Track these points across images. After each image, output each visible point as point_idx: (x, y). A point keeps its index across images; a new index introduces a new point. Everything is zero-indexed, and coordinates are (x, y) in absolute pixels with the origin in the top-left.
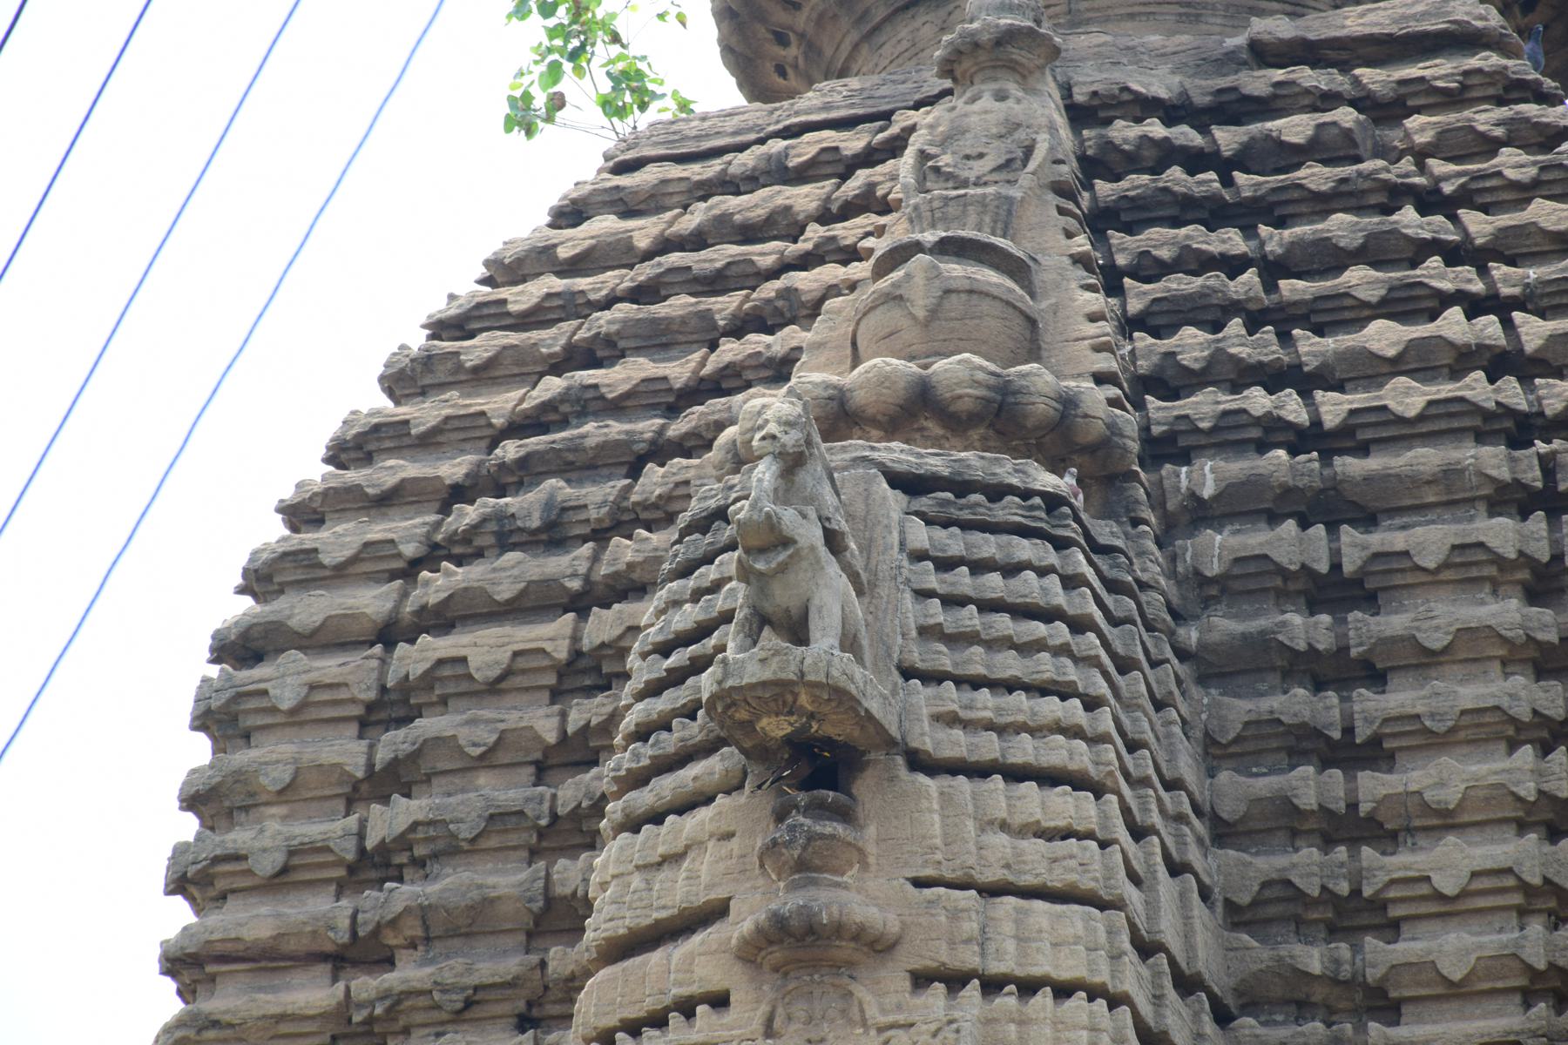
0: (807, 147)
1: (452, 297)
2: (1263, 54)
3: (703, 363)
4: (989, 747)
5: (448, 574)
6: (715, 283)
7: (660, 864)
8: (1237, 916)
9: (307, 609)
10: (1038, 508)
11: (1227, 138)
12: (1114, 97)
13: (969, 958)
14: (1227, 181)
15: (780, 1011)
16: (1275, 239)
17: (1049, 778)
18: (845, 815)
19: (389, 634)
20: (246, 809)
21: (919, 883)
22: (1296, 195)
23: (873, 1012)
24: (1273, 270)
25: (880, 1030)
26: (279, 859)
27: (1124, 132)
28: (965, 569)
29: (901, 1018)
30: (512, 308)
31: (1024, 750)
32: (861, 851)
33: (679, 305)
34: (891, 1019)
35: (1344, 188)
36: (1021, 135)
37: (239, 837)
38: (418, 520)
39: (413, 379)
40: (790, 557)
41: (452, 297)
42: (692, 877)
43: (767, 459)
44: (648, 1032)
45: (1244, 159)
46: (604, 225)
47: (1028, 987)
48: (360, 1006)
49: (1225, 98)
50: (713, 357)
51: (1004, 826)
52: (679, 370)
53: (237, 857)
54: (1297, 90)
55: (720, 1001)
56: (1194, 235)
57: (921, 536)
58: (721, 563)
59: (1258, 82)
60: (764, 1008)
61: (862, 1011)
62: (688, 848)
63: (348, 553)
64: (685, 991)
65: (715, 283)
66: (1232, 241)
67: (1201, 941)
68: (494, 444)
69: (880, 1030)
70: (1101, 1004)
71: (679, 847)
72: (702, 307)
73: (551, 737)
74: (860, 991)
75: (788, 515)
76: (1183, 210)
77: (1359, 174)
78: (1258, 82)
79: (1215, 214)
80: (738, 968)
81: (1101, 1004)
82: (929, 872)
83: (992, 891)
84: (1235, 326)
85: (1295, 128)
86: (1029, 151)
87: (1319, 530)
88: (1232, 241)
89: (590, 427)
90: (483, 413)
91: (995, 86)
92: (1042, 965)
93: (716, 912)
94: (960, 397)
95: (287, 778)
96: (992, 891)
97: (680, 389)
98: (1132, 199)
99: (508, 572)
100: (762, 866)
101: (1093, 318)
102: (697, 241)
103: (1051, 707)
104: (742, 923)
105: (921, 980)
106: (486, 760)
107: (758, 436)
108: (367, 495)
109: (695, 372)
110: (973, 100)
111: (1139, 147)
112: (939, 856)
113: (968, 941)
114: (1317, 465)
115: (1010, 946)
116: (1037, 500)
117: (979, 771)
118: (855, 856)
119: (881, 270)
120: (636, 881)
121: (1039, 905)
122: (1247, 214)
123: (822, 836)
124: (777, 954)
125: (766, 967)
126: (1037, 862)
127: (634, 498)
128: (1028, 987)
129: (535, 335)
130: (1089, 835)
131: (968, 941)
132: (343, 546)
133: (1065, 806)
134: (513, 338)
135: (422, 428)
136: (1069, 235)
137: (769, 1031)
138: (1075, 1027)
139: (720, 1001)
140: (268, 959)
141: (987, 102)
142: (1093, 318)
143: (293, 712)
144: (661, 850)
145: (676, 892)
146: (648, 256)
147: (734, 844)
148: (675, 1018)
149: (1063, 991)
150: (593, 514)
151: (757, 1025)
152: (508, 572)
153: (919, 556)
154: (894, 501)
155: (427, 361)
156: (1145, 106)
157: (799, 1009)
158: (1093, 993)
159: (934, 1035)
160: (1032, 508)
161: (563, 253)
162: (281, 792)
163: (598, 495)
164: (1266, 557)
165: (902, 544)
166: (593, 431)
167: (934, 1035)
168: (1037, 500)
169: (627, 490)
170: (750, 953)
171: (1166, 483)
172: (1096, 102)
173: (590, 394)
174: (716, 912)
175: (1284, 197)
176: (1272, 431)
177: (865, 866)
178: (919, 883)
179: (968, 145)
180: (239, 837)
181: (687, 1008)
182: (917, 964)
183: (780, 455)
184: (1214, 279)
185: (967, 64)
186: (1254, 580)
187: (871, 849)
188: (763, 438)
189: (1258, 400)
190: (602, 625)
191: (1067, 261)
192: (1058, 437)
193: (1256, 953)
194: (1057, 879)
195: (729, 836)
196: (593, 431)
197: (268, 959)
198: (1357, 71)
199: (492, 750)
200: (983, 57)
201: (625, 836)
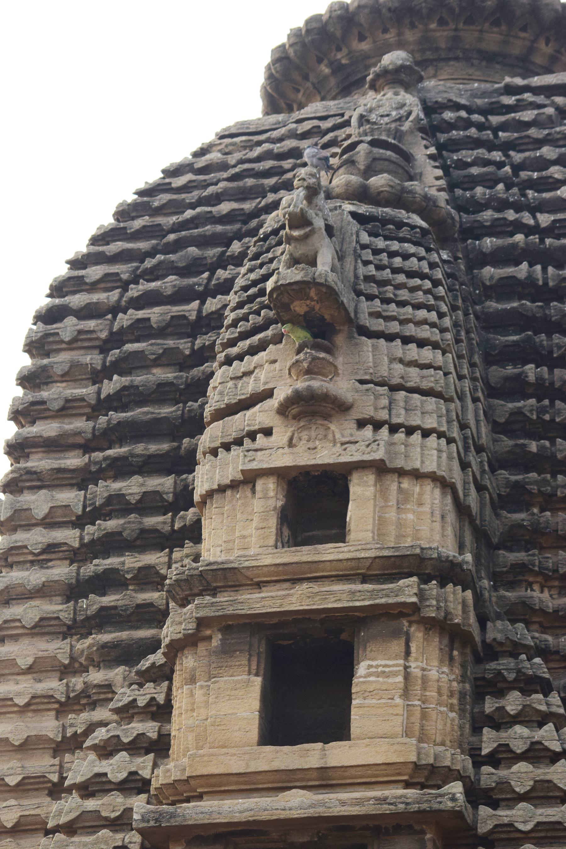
0: (307, 126)
1: (146, 183)
2: (510, 90)
3: (260, 202)
4: (394, 327)
5: (143, 284)
6: (267, 174)
7: (240, 378)
8: (497, 428)
9: (77, 300)
10: (418, 233)
11: (495, 120)
12: (444, 104)
13: (383, 415)
14: (496, 136)
15: (296, 435)
16: (517, 157)
17: (421, 343)
18: (328, 351)
19: (116, 310)
20: (47, 384)
21: (362, 382)
22: (527, 140)
23: (338, 436)
24: (517, 168)
25: (342, 444)
26: (61, 403)
27: (448, 115)
28: (385, 254)
29: (352, 439)
30: (173, 185)
31: (411, 330)
32: (335, 367)
33: (250, 182)
34: (347, 439)
35: (549, 137)
36: (406, 108)
37: (45, 394)
38: (129, 265)
39: (129, 213)
40: (310, 231)
41: (146, 183)
42: (257, 380)
43: (301, 189)
44: (233, 447)
45: (503, 127)
46: (214, 156)
47: (410, 431)
48: (95, 463)
49: (494, 106)
50: (264, 200)
51: (401, 361)
52: (248, 206)
53: (43, 402)
54: (526, 103)
55: (268, 432)
56: (481, 152)
57: (365, 238)
58: (274, 251)
59: (509, 100)
60: (289, 434)
61: (334, 436)
62: (255, 368)
63: (98, 277)
64: (252, 428)
65: (267, 174)
66: (497, 156)
67: (484, 434)
68: (165, 236)
69: (342, 444)
70: (443, 441)
71: (252, 368)
72: (260, 183)
73: (187, 352)
74: (333, 427)
75: (311, 213)
76: (477, 143)
77: (556, 132)
78: (509, 100)
79: (491, 147)
80: (277, 417)
81: (443, 441)
82: (367, 377)
83: (394, 388)
84: (501, 186)
85: (527, 115)
86: (409, 113)
87: (538, 267)
88: (497, 156)
89: (208, 227)
90: (160, 225)
91: (394, 90)
92: (416, 421)
93: (268, 394)
94: (382, 191)
95: (66, 369)
96: (394, 388)
97: (249, 214)
98: (454, 140)
99: (170, 283)
100: (289, 370)
101: (438, 178)
102: (258, 159)
103: (422, 314)
104: (282, 393)
105: (361, 424)
106: (157, 362)
107: (297, 179)
108: (107, 255)
109: (256, 207)
110: (384, 95)
111: (456, 121)
112: (371, 371)
113: (383, 408)
114: (537, 240)
115: (403, 412)
116: (418, 230)
117: (390, 338)
118: (333, 369)
119: (344, 152)
120: (230, 384)
121: (416, 396)
122: (506, 147)
123: (319, 358)
124: (295, 410)
125: (290, 417)
126: (414, 376)
127: (228, 254)
128: (410, 431)
129: (183, 196)
130: (439, 368)
131: (383, 408)
132: (97, 274)
133: (427, 355)
134: (175, 197)
135: (132, 230)
136: (426, 147)
137: (291, 444)
138: (432, 449)
139: (268, 432)
140: (53, 445)
141: (390, 94)
142: (438, 178)
143: (70, 343)
144: (242, 370)
145: (250, 386)
146: (235, 166)
147: (277, 365)
148: (247, 441)
149: (426, 433)
150: (209, 261)
151: (285, 439)
152: (170, 283)
153: (364, 247)
154: (354, 226)
155: (135, 206)
156: (457, 107)
157: (305, 435)
158: (441, 435)
159: (368, 446)
160: (416, 233)
161: (196, 166)
162: (63, 376)
163: (212, 253)
164: (514, 277)
165: (357, 242)
166: (209, 229)
167: (368, 446)
168: (418, 230)
169: (225, 252)
170: (283, 410)
171: (469, 247)
172: (436, 106)
173: (209, 215)
174: (268, 394)
175: (520, 141)
176: (518, 227)
177: (336, 373)
178: (362, 382)
179: (381, 111)
180: (45, 394)
181: (252, 436)
182: (360, 416)
183: (308, 188)
184: (490, 169)
185: (381, 81)
186: (507, 288)
187: (340, 367)
188: (299, 180)
189: (511, 215)
190: (212, 305)
191: (426, 157)
192: (426, 207)
193: (507, 443)
194: (425, 385)
195: (275, 361)
196: (209, 229)
197: (53, 445)
198: (553, 98)
199: (160, 356)
200: (389, 77)
201: (224, 368)
